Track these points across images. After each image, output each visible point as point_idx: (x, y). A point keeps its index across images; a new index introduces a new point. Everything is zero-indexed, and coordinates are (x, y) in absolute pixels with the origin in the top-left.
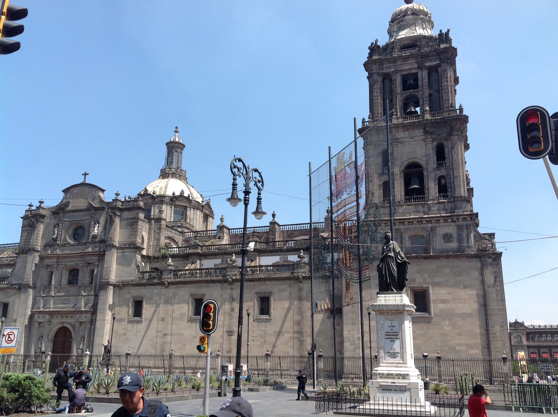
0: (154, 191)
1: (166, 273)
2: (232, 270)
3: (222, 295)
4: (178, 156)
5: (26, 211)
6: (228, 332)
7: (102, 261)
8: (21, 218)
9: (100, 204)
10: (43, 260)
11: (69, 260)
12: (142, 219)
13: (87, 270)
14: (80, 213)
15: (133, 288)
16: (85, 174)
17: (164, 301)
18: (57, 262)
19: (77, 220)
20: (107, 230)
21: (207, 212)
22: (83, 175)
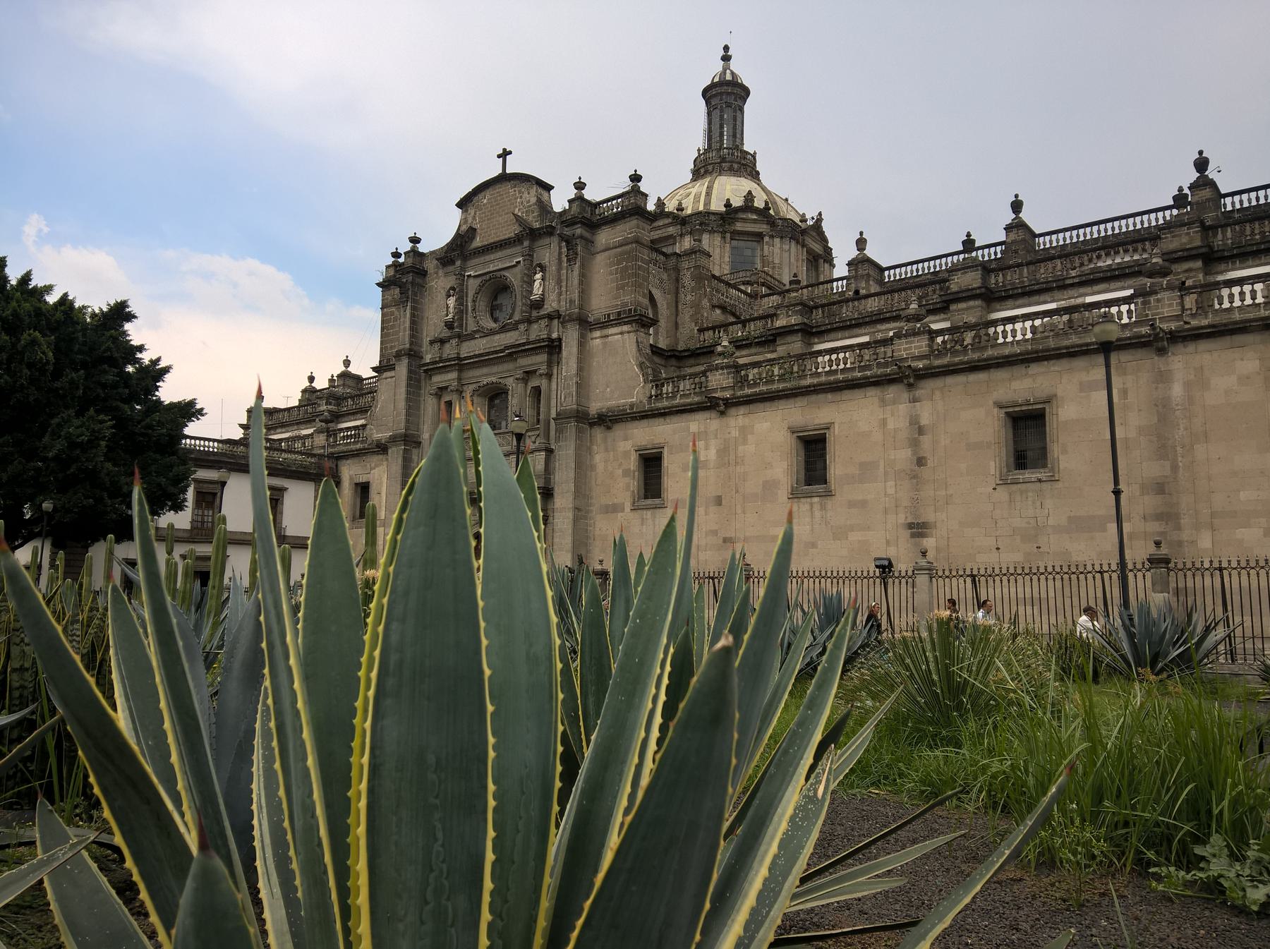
0: (680, 204)
1: (718, 377)
2: (912, 342)
3: (884, 423)
4: (735, 119)
5: (388, 267)
6: (910, 526)
7: (558, 363)
8: (378, 284)
9: (542, 221)
10: (431, 376)
11: (485, 370)
12: (645, 242)
13: (526, 391)
14: (499, 254)
15: (637, 423)
16: (505, 154)
17: (718, 451)
18: (459, 379)
19: (495, 269)
20: (564, 284)
21: (817, 248)
22: (499, 156)
